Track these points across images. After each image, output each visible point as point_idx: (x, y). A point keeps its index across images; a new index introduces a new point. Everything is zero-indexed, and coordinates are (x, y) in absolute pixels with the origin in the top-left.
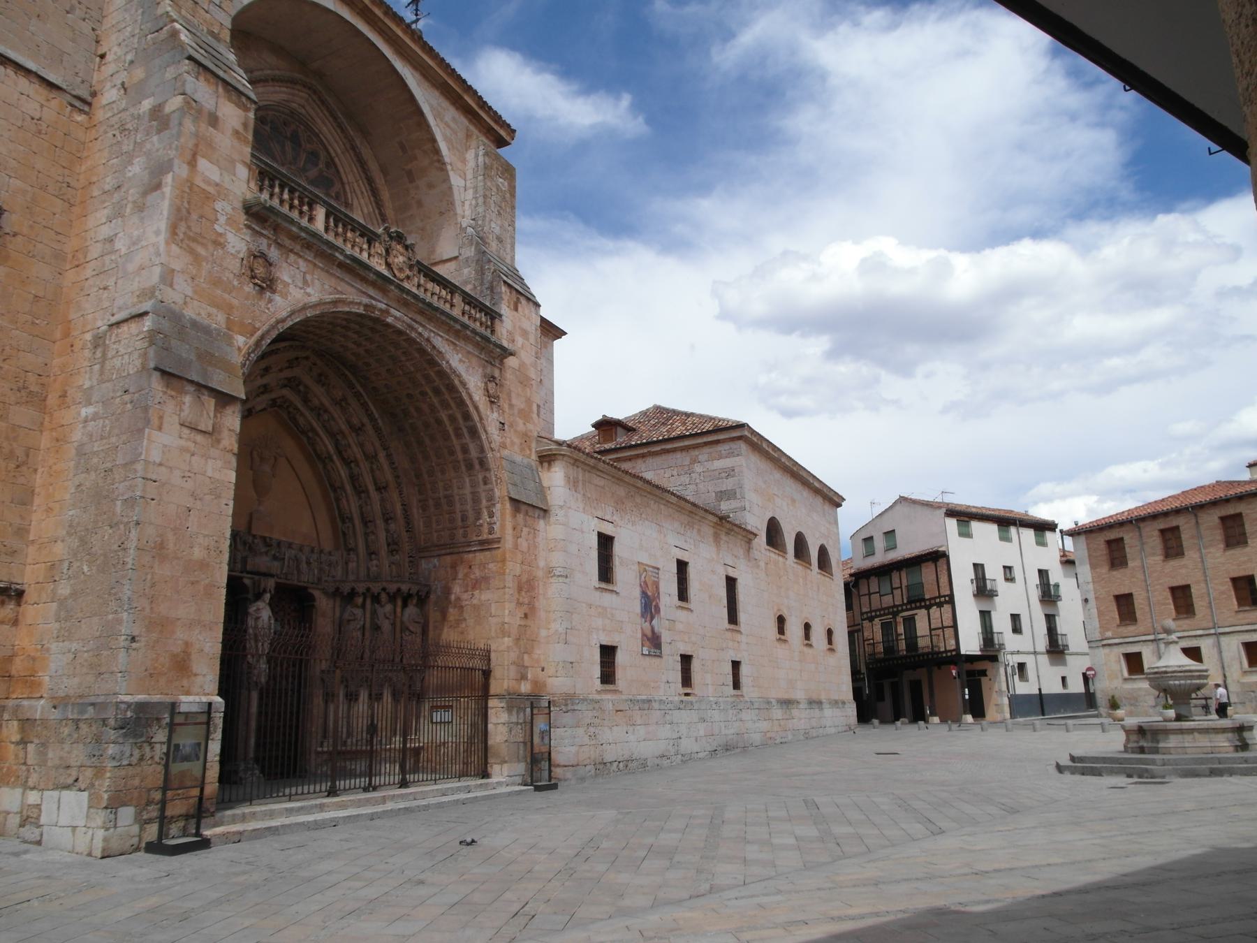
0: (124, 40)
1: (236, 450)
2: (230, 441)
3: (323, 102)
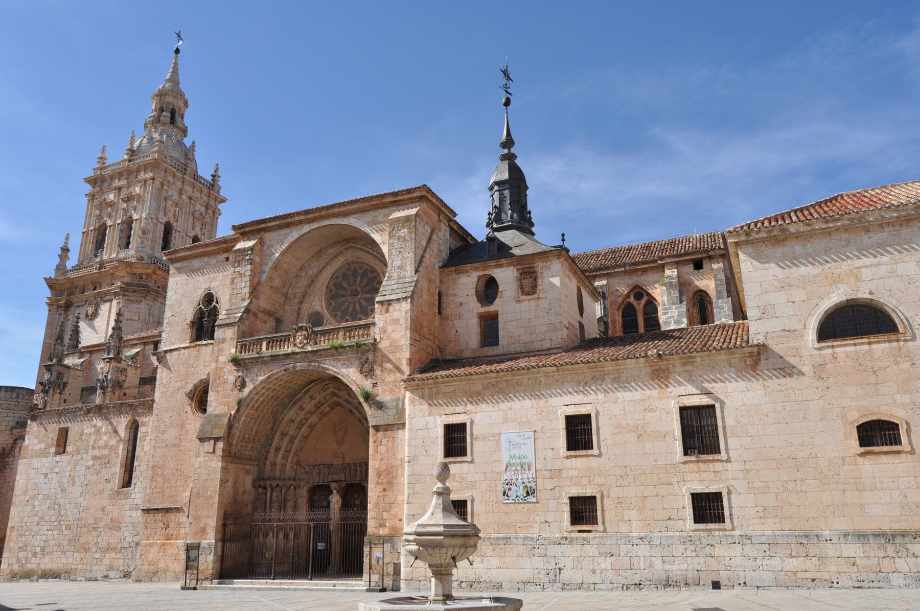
2: (219, 452)
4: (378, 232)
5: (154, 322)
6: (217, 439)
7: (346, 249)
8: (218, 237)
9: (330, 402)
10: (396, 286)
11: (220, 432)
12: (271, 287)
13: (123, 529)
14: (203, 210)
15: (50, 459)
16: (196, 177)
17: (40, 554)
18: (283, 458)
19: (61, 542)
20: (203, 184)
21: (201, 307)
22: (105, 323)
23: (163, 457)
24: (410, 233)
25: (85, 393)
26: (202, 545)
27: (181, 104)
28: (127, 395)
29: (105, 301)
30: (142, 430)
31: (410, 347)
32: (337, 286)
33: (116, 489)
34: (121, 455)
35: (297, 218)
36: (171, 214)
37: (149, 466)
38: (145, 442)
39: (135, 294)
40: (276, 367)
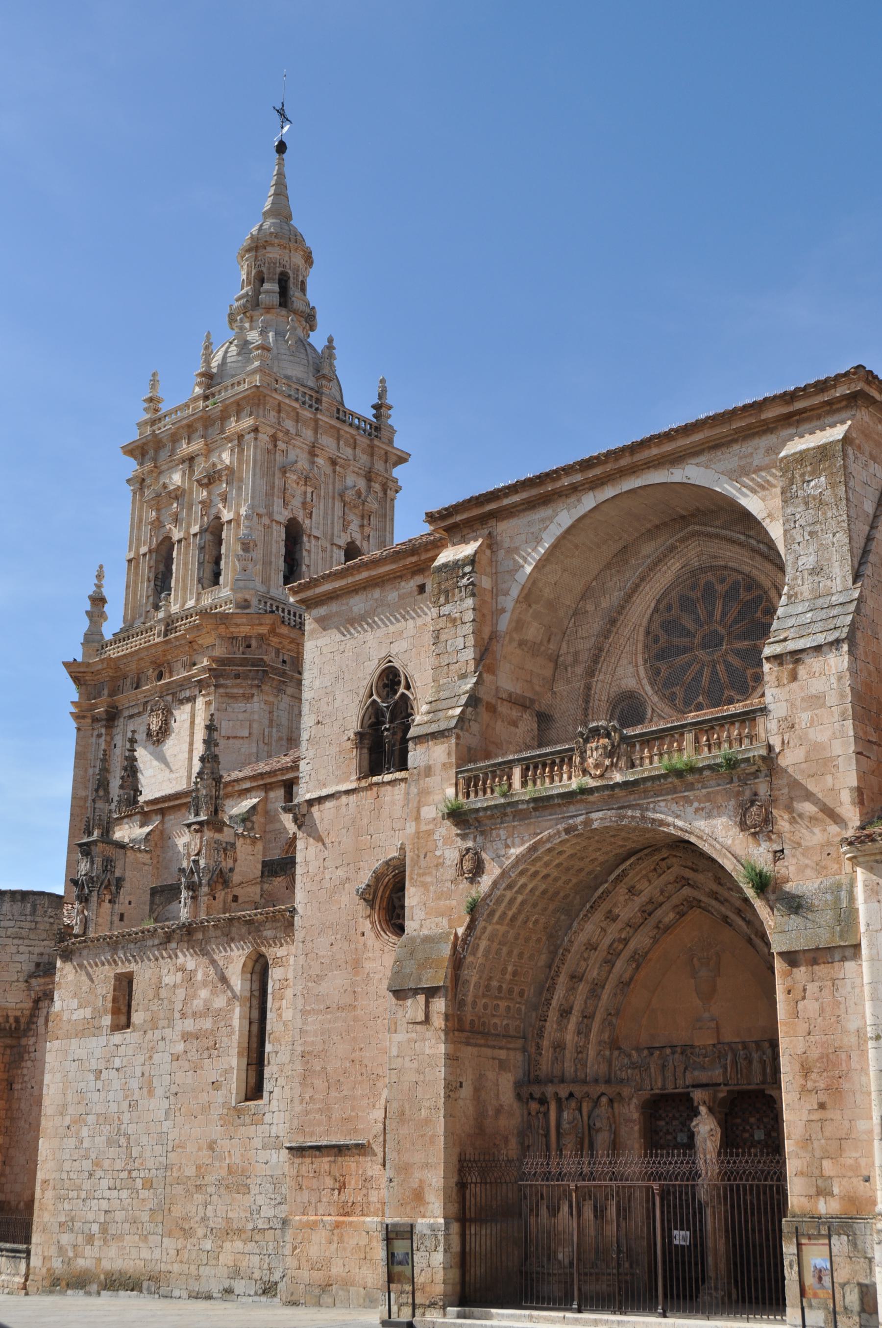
1: (443, 1027)
2: (438, 1021)
3: (710, 536)
4: (754, 491)
5: (281, 739)
6: (431, 993)
7: (683, 540)
8: (397, 541)
9: (675, 900)
10: (809, 615)
11: (437, 977)
12: (522, 644)
13: (254, 1189)
14: (362, 484)
15: (102, 1040)
16: (342, 414)
17: (100, 1239)
18: (579, 1033)
19: (137, 1213)
20: (358, 428)
21: (374, 701)
22: (186, 747)
23: (322, 1034)
24: (833, 485)
25: (157, 900)
26: (418, 1229)
27: (298, 259)
28: (240, 900)
29: (182, 702)
30: (275, 974)
31: (857, 761)
32: (670, 626)
33: (233, 1105)
34: (237, 1029)
35: (566, 481)
36: (296, 502)
37: (296, 1053)
38: (284, 1001)
39: (238, 681)
40: (547, 824)
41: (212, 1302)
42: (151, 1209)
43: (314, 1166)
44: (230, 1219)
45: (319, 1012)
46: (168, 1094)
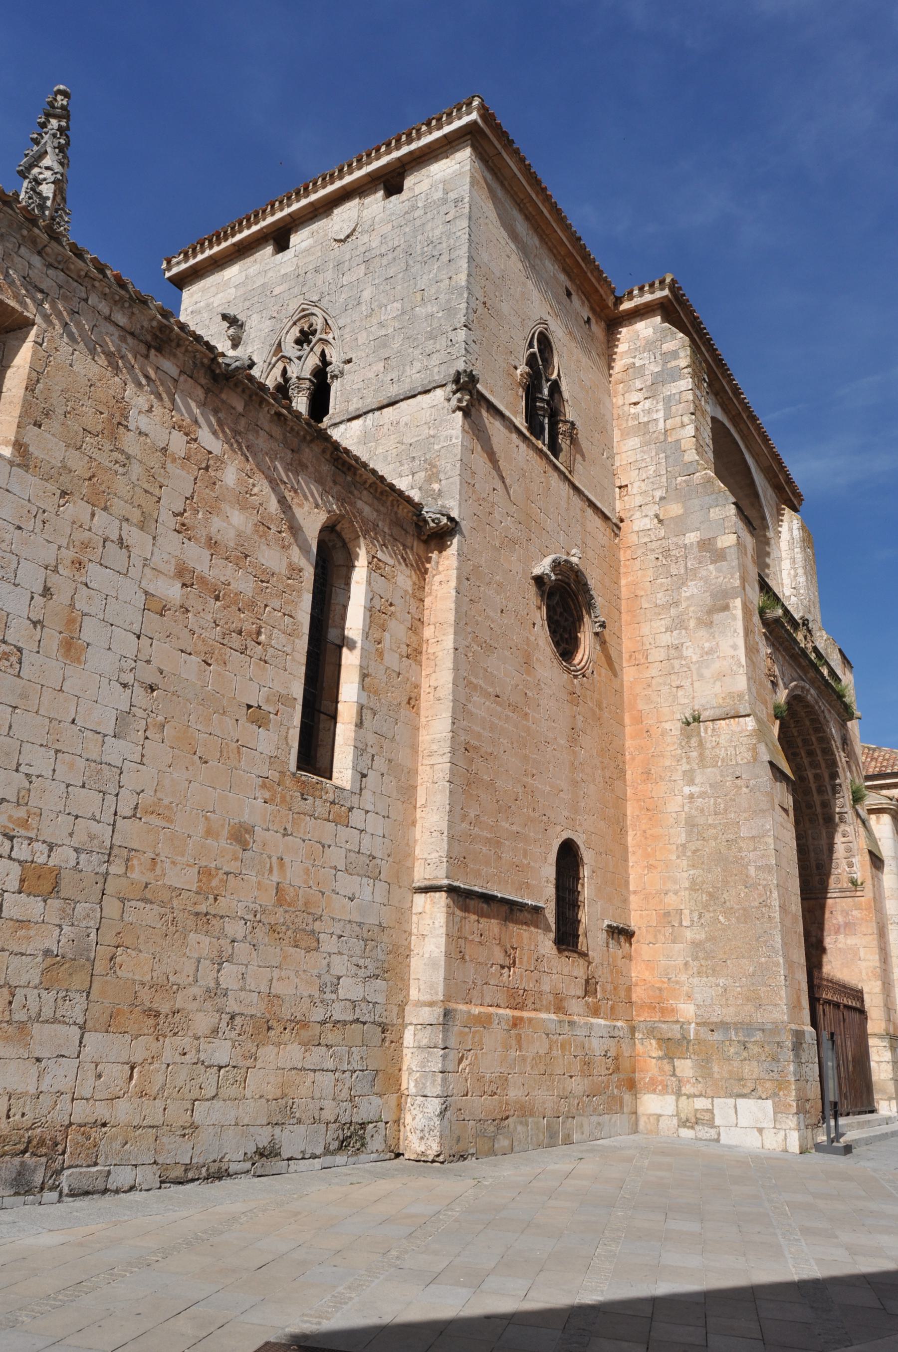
0: (648, 478)
13: (329, 944)
41: (226, 1183)
42: (47, 953)
43: (481, 926)
44: (277, 996)
45: (487, 695)
46: (128, 678)
